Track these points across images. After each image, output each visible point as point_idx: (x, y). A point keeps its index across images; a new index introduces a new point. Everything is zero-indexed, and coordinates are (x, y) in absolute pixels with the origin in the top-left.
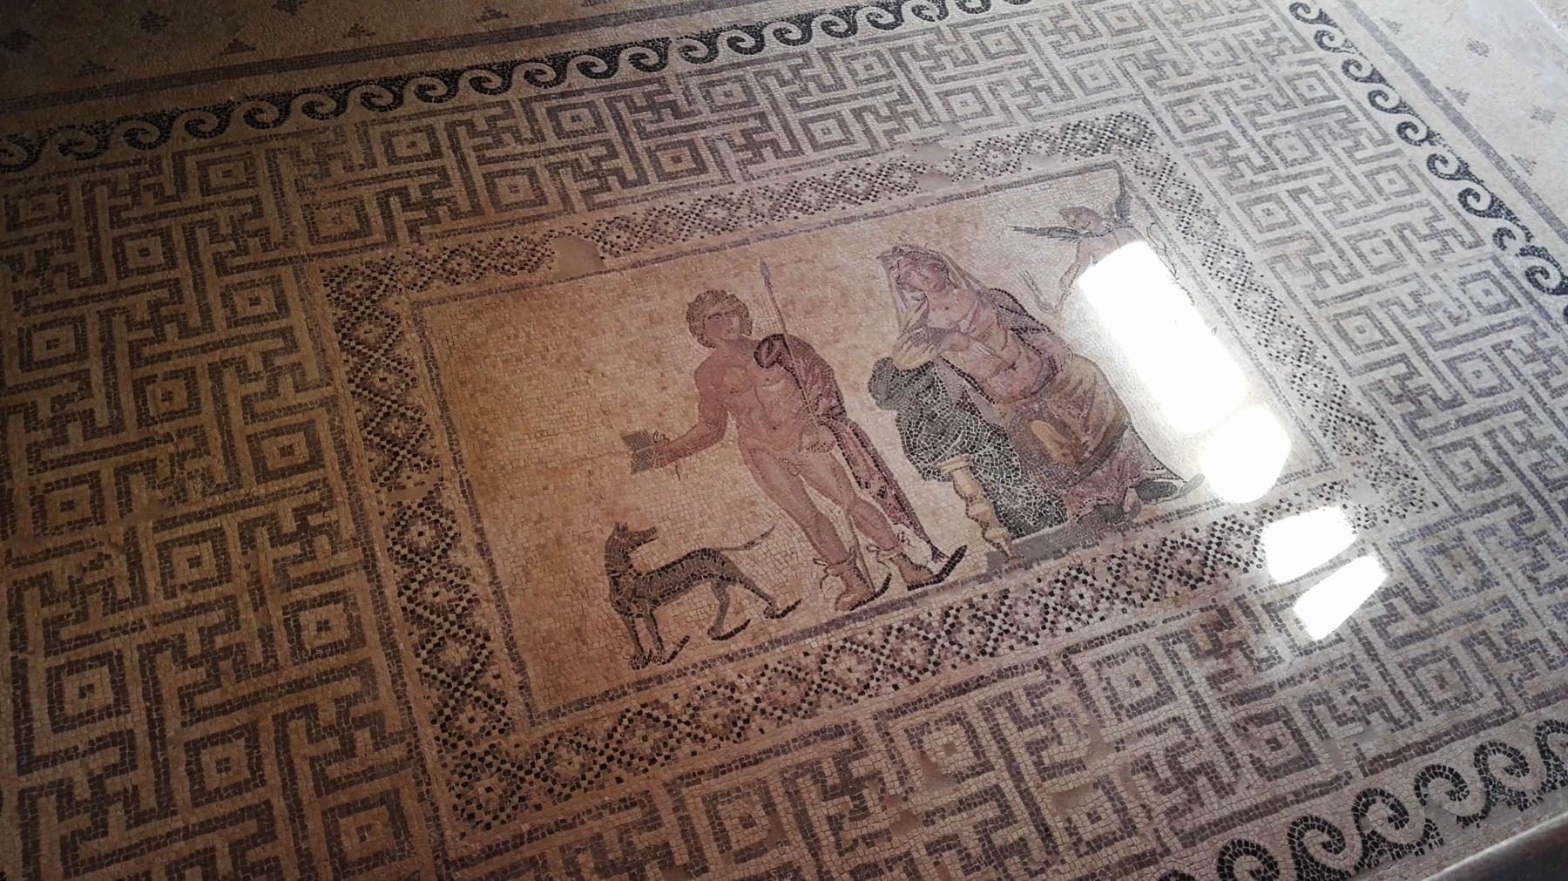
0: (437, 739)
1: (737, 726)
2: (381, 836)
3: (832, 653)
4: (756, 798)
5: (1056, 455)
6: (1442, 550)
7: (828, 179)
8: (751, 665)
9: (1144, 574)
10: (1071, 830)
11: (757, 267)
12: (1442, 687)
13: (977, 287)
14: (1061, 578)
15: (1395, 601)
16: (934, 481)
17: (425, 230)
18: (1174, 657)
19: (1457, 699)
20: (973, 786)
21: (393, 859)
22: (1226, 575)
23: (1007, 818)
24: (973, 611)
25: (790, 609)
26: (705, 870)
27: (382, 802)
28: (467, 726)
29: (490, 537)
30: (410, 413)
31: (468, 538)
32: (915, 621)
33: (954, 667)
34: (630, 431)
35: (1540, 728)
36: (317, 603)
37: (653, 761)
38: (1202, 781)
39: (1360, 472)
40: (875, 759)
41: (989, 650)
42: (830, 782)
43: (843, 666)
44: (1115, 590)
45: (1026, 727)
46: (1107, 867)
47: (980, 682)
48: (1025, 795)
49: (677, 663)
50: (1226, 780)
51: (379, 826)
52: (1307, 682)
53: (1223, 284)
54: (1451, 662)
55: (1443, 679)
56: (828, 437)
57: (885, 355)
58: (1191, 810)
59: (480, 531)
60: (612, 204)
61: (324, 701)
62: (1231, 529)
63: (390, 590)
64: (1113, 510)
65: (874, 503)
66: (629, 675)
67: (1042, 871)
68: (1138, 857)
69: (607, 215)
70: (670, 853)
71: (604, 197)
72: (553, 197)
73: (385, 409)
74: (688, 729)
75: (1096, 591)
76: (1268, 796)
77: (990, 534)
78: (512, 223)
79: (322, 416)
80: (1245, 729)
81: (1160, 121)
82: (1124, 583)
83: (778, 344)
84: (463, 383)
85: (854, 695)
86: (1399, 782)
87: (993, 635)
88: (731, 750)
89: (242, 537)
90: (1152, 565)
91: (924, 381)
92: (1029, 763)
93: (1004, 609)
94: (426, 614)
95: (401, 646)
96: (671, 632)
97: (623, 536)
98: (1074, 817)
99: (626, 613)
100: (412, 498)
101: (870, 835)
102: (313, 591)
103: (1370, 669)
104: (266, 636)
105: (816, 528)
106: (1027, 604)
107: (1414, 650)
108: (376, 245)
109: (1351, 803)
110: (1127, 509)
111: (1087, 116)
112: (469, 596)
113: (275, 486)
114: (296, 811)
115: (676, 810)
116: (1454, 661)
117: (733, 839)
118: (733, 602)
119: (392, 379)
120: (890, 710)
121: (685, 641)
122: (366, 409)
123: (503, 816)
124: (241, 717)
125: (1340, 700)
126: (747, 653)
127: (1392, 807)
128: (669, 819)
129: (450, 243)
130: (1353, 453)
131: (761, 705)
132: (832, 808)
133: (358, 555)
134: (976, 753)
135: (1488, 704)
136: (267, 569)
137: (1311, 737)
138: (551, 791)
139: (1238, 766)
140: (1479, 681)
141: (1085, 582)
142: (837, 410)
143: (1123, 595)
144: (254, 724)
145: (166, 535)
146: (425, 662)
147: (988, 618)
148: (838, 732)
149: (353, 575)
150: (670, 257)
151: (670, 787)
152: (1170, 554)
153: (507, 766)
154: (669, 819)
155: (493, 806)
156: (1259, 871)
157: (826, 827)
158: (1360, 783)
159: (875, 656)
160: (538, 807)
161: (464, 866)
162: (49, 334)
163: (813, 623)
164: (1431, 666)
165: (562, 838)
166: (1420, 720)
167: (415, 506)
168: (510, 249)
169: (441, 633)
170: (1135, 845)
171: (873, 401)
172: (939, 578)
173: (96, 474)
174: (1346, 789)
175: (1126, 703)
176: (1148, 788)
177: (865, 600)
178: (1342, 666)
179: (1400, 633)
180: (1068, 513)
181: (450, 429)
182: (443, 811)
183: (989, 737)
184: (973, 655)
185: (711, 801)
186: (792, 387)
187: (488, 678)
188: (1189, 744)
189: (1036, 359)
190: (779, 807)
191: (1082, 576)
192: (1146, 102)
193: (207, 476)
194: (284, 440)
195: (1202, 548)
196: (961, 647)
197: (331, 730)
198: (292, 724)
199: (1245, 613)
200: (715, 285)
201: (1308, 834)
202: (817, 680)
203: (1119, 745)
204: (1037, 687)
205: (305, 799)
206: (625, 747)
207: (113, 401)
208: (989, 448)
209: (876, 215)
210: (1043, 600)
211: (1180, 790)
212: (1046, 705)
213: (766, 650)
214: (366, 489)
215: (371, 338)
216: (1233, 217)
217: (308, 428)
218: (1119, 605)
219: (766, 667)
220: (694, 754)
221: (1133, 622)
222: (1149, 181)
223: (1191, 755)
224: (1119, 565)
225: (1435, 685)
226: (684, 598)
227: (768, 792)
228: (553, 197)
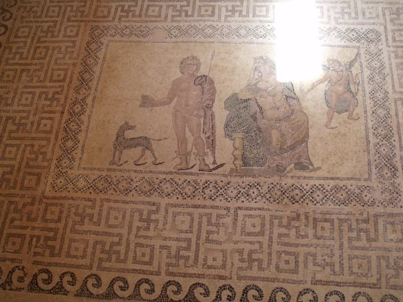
0: (56, 164)
1: (127, 191)
2: (33, 184)
3: (165, 181)
4: (122, 213)
5: (274, 144)
6: (392, 223)
7: (252, 27)
8: (141, 175)
9: (279, 193)
10: (205, 260)
11: (211, 52)
12: (359, 268)
14: (251, 184)
15: (362, 234)
17: (123, 19)
18: (272, 223)
19: (361, 274)
20: (183, 236)
21: (33, 190)
22: (307, 204)
23: (188, 248)
25: (160, 163)
26: (99, 225)
27: (37, 175)
28: (64, 164)
29: (93, 114)
30: (92, 73)
31: (88, 112)
32: (195, 182)
33: (199, 199)
34: (145, 94)
35: (386, 295)
36: (47, 119)
37: (101, 192)
38: (256, 263)
39: (380, 185)
40: (160, 216)
41: (213, 198)
42: (143, 217)
43: (166, 186)
44: (266, 195)
45: (210, 225)
46: (209, 275)
47: (204, 207)
48: (198, 245)
49: (121, 168)
50: (263, 266)
51: (34, 181)
52: (312, 248)
53: (372, 102)
54: (368, 262)
55: (361, 265)
56: (202, 113)
57: (236, 92)
58: (246, 270)
59: (91, 112)
60: (179, 21)
61: (37, 143)
62: (319, 189)
63: (63, 121)
64: (282, 169)
65: (204, 139)
66: (107, 166)
67: (189, 267)
68: (221, 276)
69: (175, 24)
70: (93, 217)
71: (178, 18)
72: (163, 16)
73: (86, 70)
74: (114, 187)
75: (260, 193)
76: (274, 277)
78: (147, 22)
79: (71, 68)
80: (281, 254)
81: (386, 35)
82: (270, 194)
83: (204, 78)
84: (109, 67)
85: (164, 196)
86: (321, 291)
87: (217, 194)
88: (122, 197)
89: (39, 96)
91: (245, 104)
92: (205, 236)
94: (68, 130)
95: (59, 137)
96: (124, 158)
97: (127, 125)
98: (208, 257)
99: (115, 148)
100: (80, 97)
101: (146, 236)
102: (48, 115)
103: (337, 253)
104: (32, 123)
105: (182, 141)
106: (234, 189)
107: (357, 253)
108: (109, 21)
109: (300, 290)
110: (288, 169)
111: (359, 27)
112: (79, 129)
113: (52, 84)
114: (19, 170)
115: (100, 207)
116: (369, 262)
117: (110, 221)
118: (145, 156)
119: (93, 61)
120: (172, 204)
121: (126, 162)
122: (82, 68)
123: (60, 190)
124: (18, 142)
125: (319, 259)
126: (141, 172)
127: (314, 297)
128: (97, 208)
129: (127, 24)
130: (382, 179)
131: (137, 188)
132: (140, 224)
133: (61, 110)
134: (190, 227)
135: (373, 280)
136: (40, 106)
137: (301, 265)
138: (74, 189)
139: (271, 264)
140: (374, 271)
141: (258, 188)
142: (210, 106)
143: (268, 197)
144: (20, 145)
145: (25, 90)
146: (62, 143)
147: (219, 188)
148: (154, 204)
149: (58, 114)
150: (186, 42)
151: (102, 200)
152: (292, 190)
153: (67, 178)
154: (97, 208)
155: (60, 186)
156: (256, 296)
157: (136, 229)
158: (308, 285)
159: (177, 187)
160: (69, 191)
161: (47, 199)
162: (24, 29)
163: (165, 170)
164: (360, 260)
165: (71, 202)
166: (343, 275)
167: (80, 99)
168: (142, 30)
169: (69, 137)
170: (222, 272)
171: (224, 106)
172: (211, 170)
173: (17, 69)
174: (302, 286)
175: (247, 231)
176: (237, 258)
177: (184, 169)
178: (327, 248)
179: (356, 245)
181: (99, 81)
182: (49, 183)
183: (197, 224)
184: (207, 198)
185: (111, 208)
186: (201, 93)
187: (73, 153)
188: (259, 251)
190: (126, 218)
191: (258, 186)
192: (385, 28)
193: (39, 77)
194: (59, 72)
195: (305, 192)
196: (205, 194)
197: (35, 153)
198: (28, 148)
199: (305, 218)
200: (195, 55)
201: (280, 293)
202: (156, 187)
203: (236, 242)
204: (221, 215)
205: (22, 167)
206: (97, 185)
207: (29, 52)
208: (253, 134)
211: (247, 263)
212: (221, 222)
213: (147, 173)
214: (71, 91)
215: (93, 49)
216: (392, 79)
217: (66, 70)
218: (264, 200)
219: (144, 178)
220: (112, 194)
221: (265, 207)
222: (368, 57)
223: (257, 255)
224: (273, 187)
225: (357, 266)
226: (133, 149)
227: (125, 213)
228: (163, 16)
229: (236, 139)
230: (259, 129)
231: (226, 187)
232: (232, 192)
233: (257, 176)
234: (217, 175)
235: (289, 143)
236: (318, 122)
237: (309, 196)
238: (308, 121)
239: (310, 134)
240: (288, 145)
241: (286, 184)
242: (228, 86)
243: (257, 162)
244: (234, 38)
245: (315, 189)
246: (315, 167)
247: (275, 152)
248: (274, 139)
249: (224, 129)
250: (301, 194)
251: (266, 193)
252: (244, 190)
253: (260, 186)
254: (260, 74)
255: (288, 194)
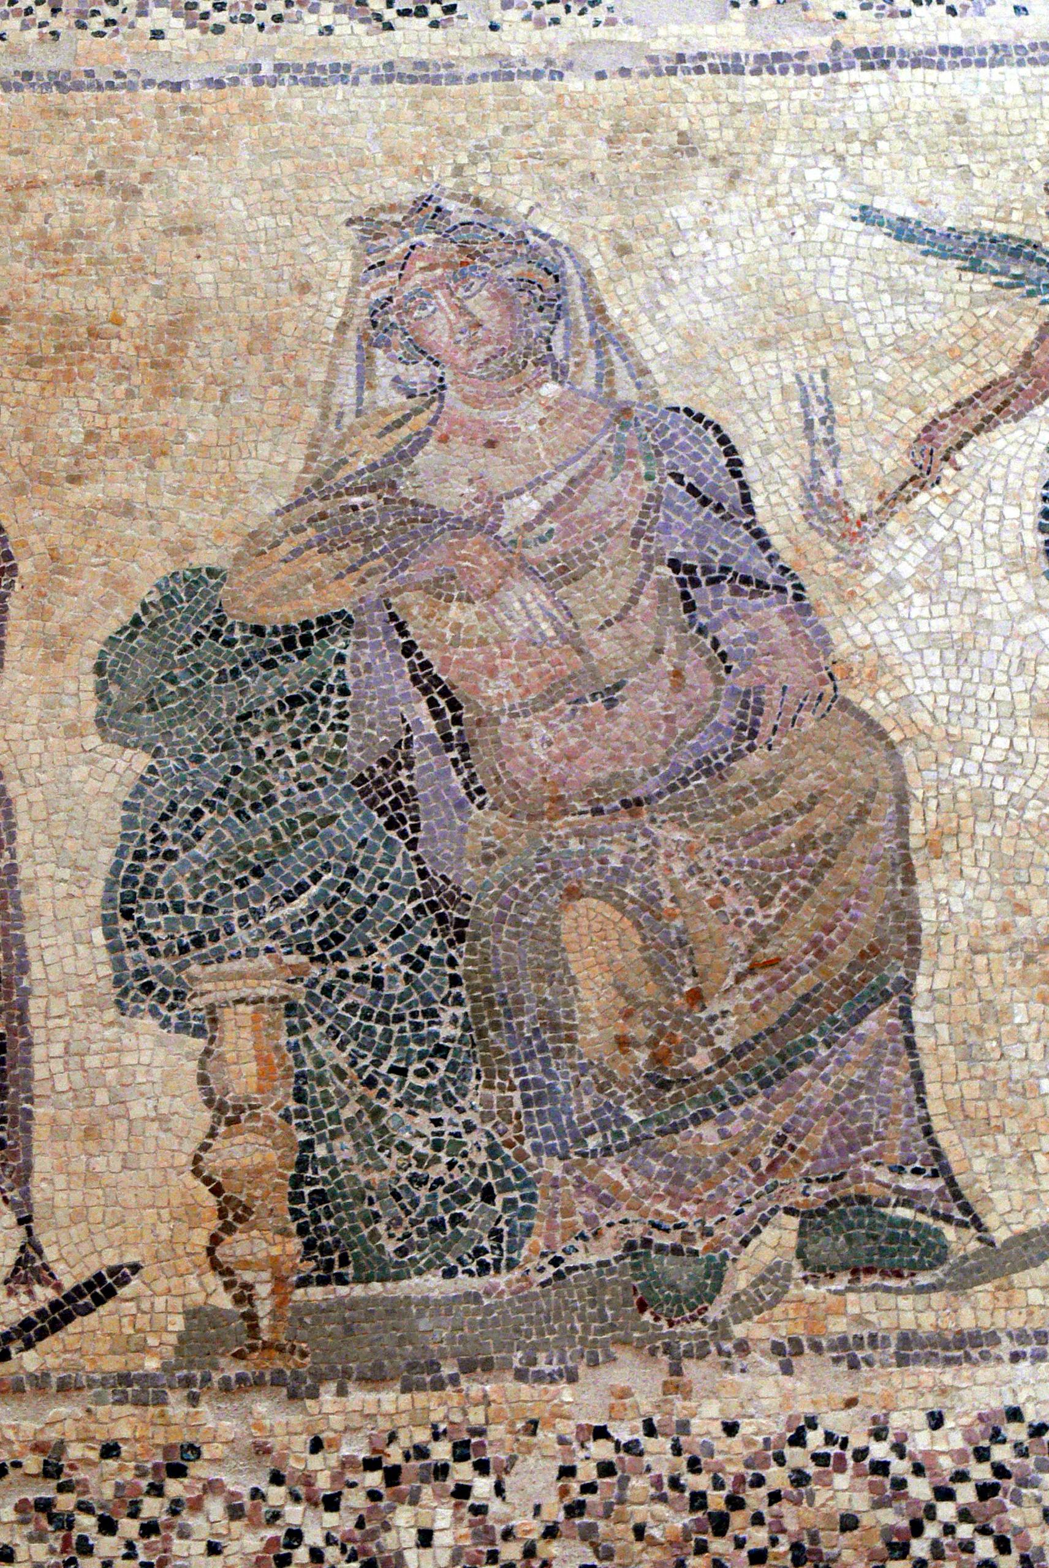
5: (593, 1037)
13: (626, 391)
14: (394, 1456)
16: (150, 1022)
24: (47, 1490)
57: (206, 557)
75: (484, 1534)
77: (239, 1246)
82: (588, 1534)
90: (716, 1501)
91: (294, 675)
93: (152, 1508)
106: (235, 1512)
147: (87, 1523)
152: (800, 1478)
180: (537, 1241)
189: (698, 676)
191: (463, 1472)
195: (920, 1489)
208: (386, 957)
209: (422, 74)
210: (294, 1514)
224: (606, 1469)
229: (227, 1015)
230: (445, 909)
231: (152, 1508)
232: (213, 1549)
233: (447, 1370)
234: (64, 1387)
235: (735, 1014)
236: (1001, 799)
237: (965, 1531)
238: (902, 797)
239: (928, 914)
240: (725, 1043)
241: (731, 1429)
242: (127, 510)
243: (437, 1225)
244: (157, 35)
245: (1022, 1452)
246: (1000, 1235)
247: (609, 1118)
248: (592, 1001)
249: (107, 922)
250: (888, 1517)
251: (551, 1532)
252: (330, 1519)
253: (482, 1467)
254: (419, 374)
255: (758, 1519)
